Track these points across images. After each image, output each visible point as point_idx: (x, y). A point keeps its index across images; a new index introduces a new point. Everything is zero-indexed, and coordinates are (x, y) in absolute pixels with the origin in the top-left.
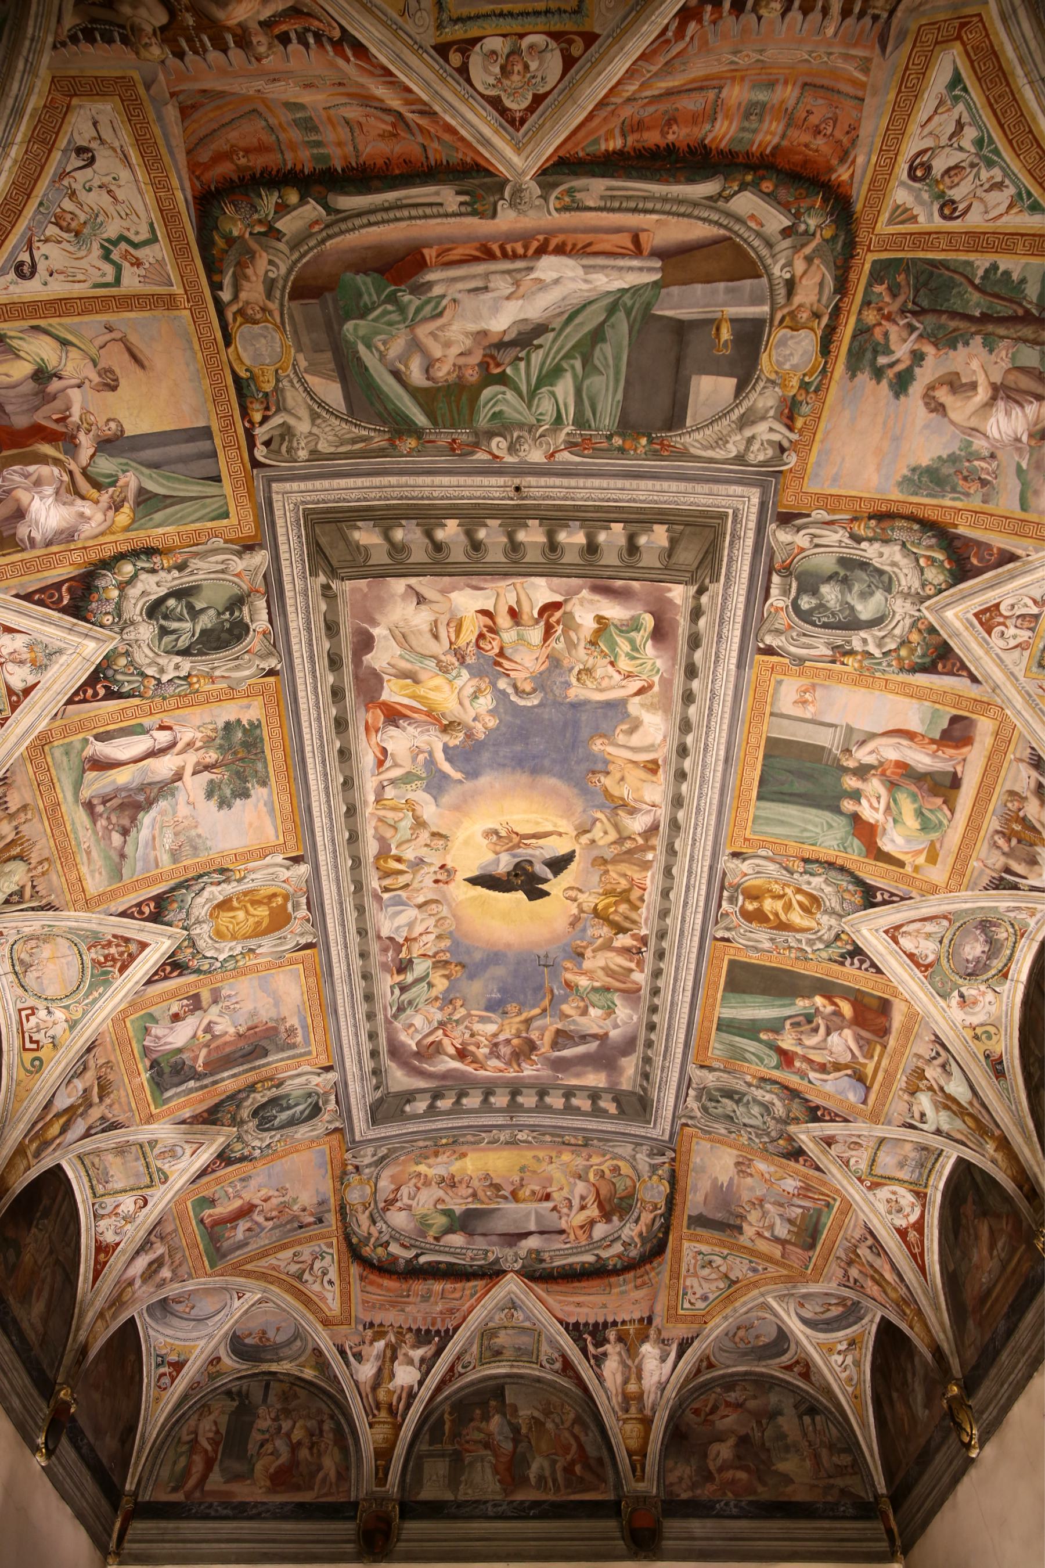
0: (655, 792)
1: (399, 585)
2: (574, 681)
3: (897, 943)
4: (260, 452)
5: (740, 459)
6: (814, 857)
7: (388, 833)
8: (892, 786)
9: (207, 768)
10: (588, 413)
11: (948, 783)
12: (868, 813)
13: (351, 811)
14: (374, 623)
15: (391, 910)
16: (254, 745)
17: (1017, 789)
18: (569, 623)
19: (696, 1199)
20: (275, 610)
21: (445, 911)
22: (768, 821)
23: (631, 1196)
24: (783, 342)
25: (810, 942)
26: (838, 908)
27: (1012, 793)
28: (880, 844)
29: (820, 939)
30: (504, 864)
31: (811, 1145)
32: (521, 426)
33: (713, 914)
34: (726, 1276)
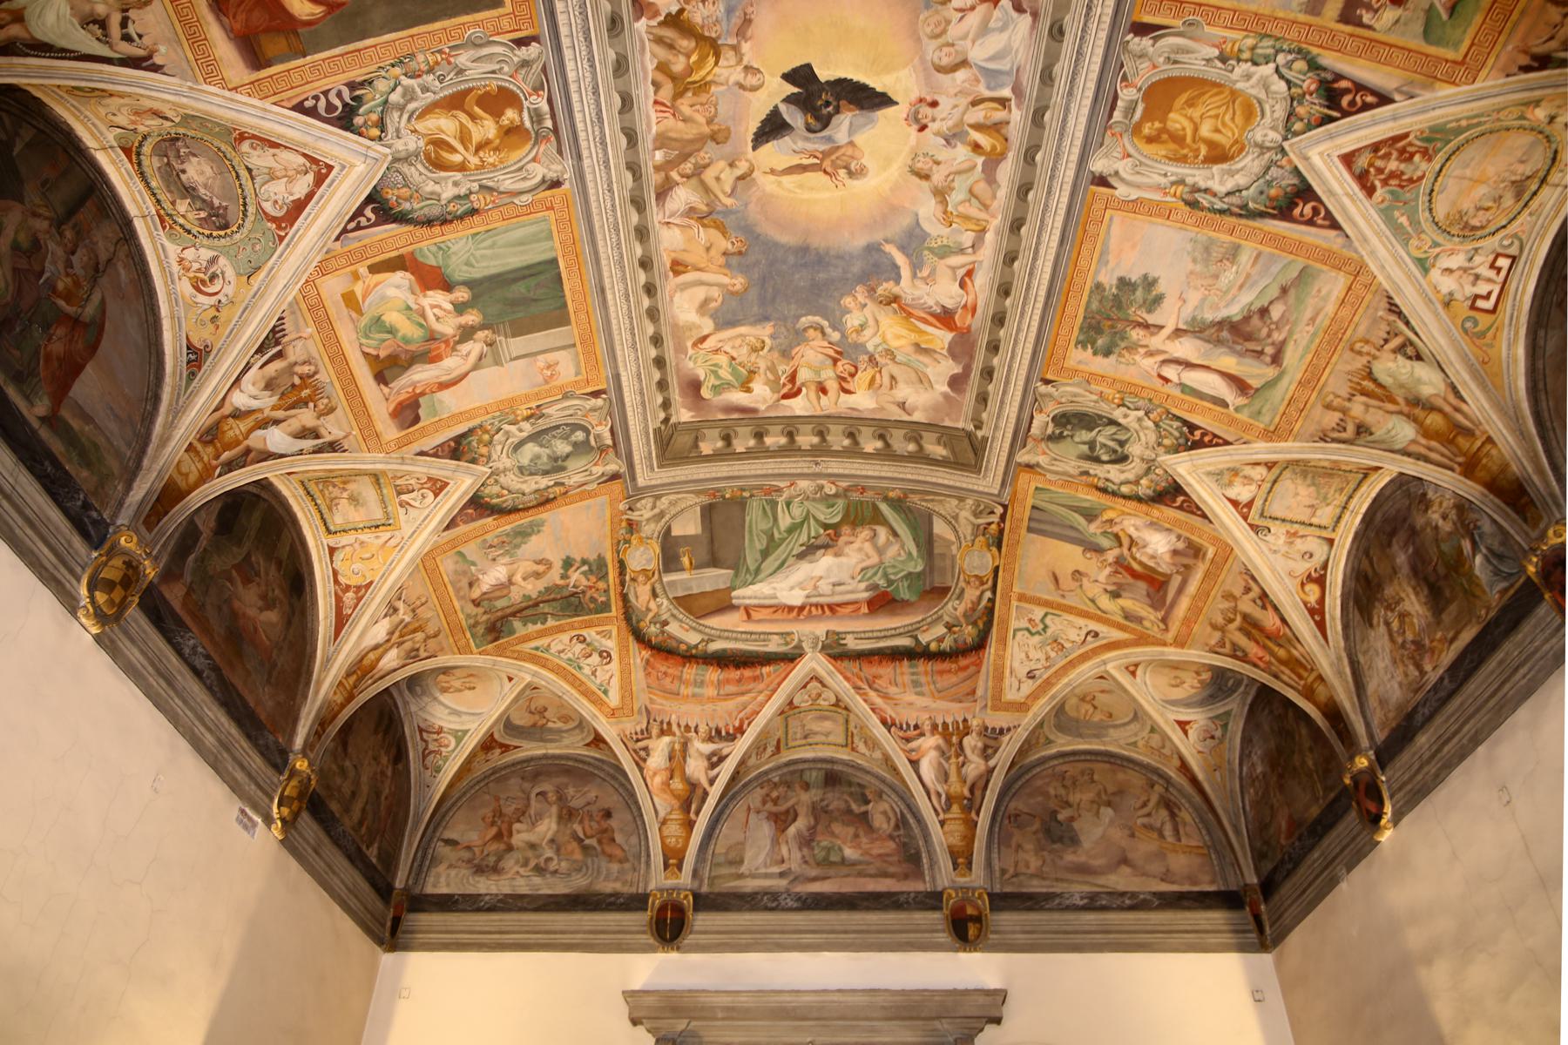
0: (670, 240)
1: (918, 417)
2: (768, 341)
3: (305, 155)
4: (999, 510)
5: (658, 497)
6: (467, 221)
7: (981, 188)
8: (432, 337)
9: (1146, 326)
10: (768, 508)
11: (387, 374)
12: (438, 300)
13: (1016, 225)
14: (946, 396)
15: (1004, 65)
16: (1090, 327)
17: (331, 417)
18: (774, 384)
20: (1025, 425)
21: (931, 46)
22: (535, 239)
24: (649, 561)
26: (405, 168)
27: (332, 410)
28: (408, 275)
29: (402, 109)
30: (844, 124)
32: (814, 500)
33: (552, 78)
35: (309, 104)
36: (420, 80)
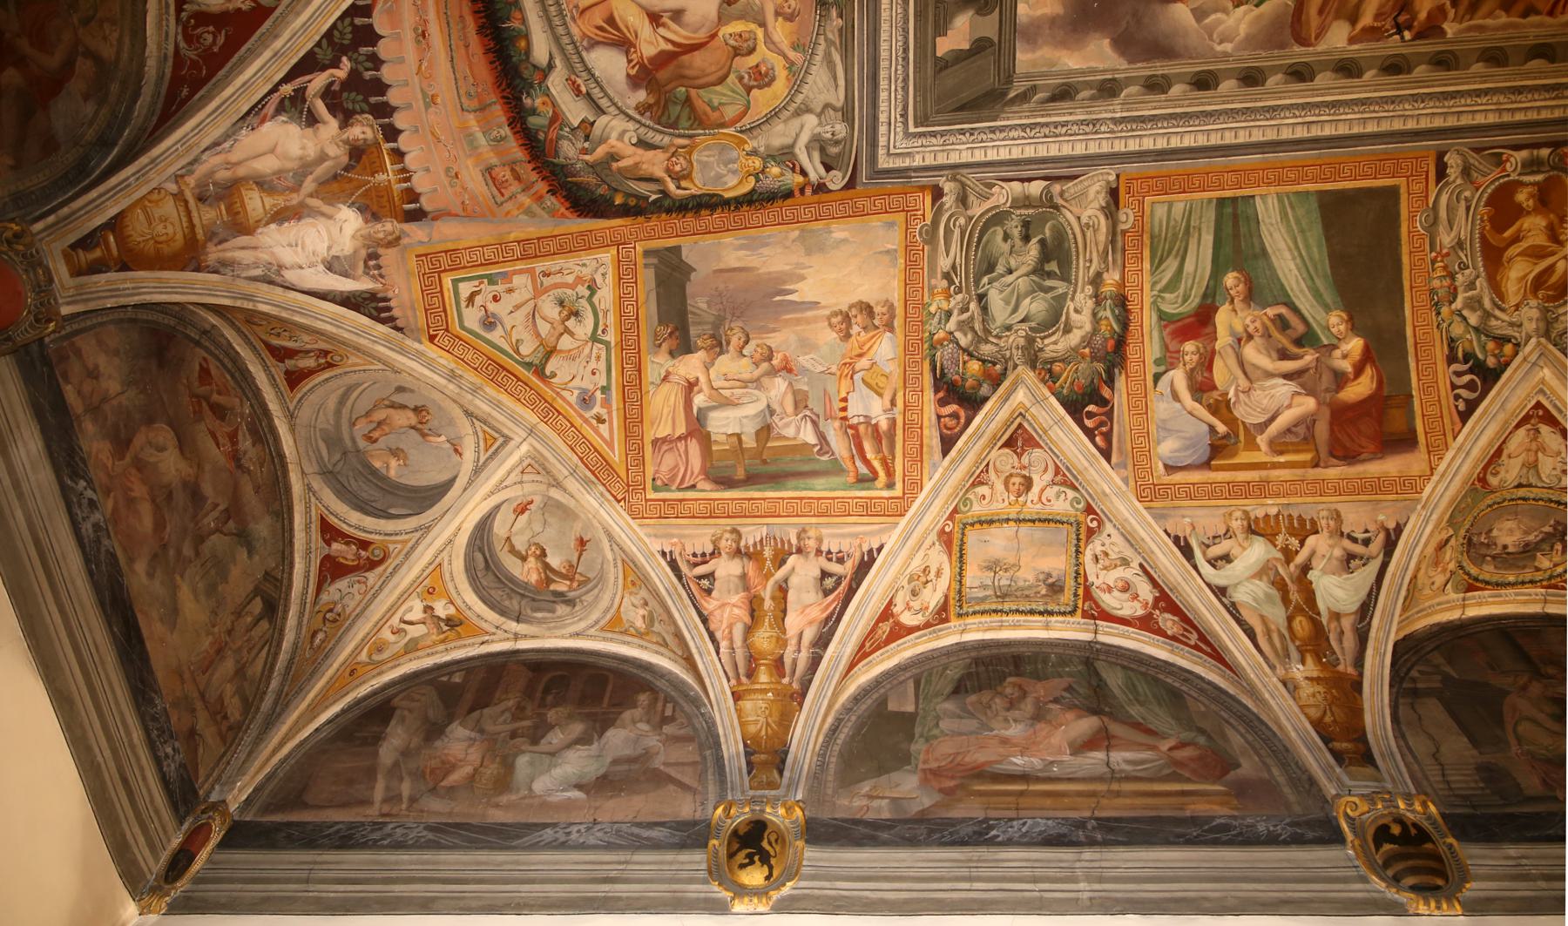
3: (1518, 426)
19: (717, 253)
23: (699, 121)
25: (1474, 304)
29: (1488, 315)
31: (1004, 414)
34: (550, 352)
35: (1462, 406)
36: (1460, 290)
